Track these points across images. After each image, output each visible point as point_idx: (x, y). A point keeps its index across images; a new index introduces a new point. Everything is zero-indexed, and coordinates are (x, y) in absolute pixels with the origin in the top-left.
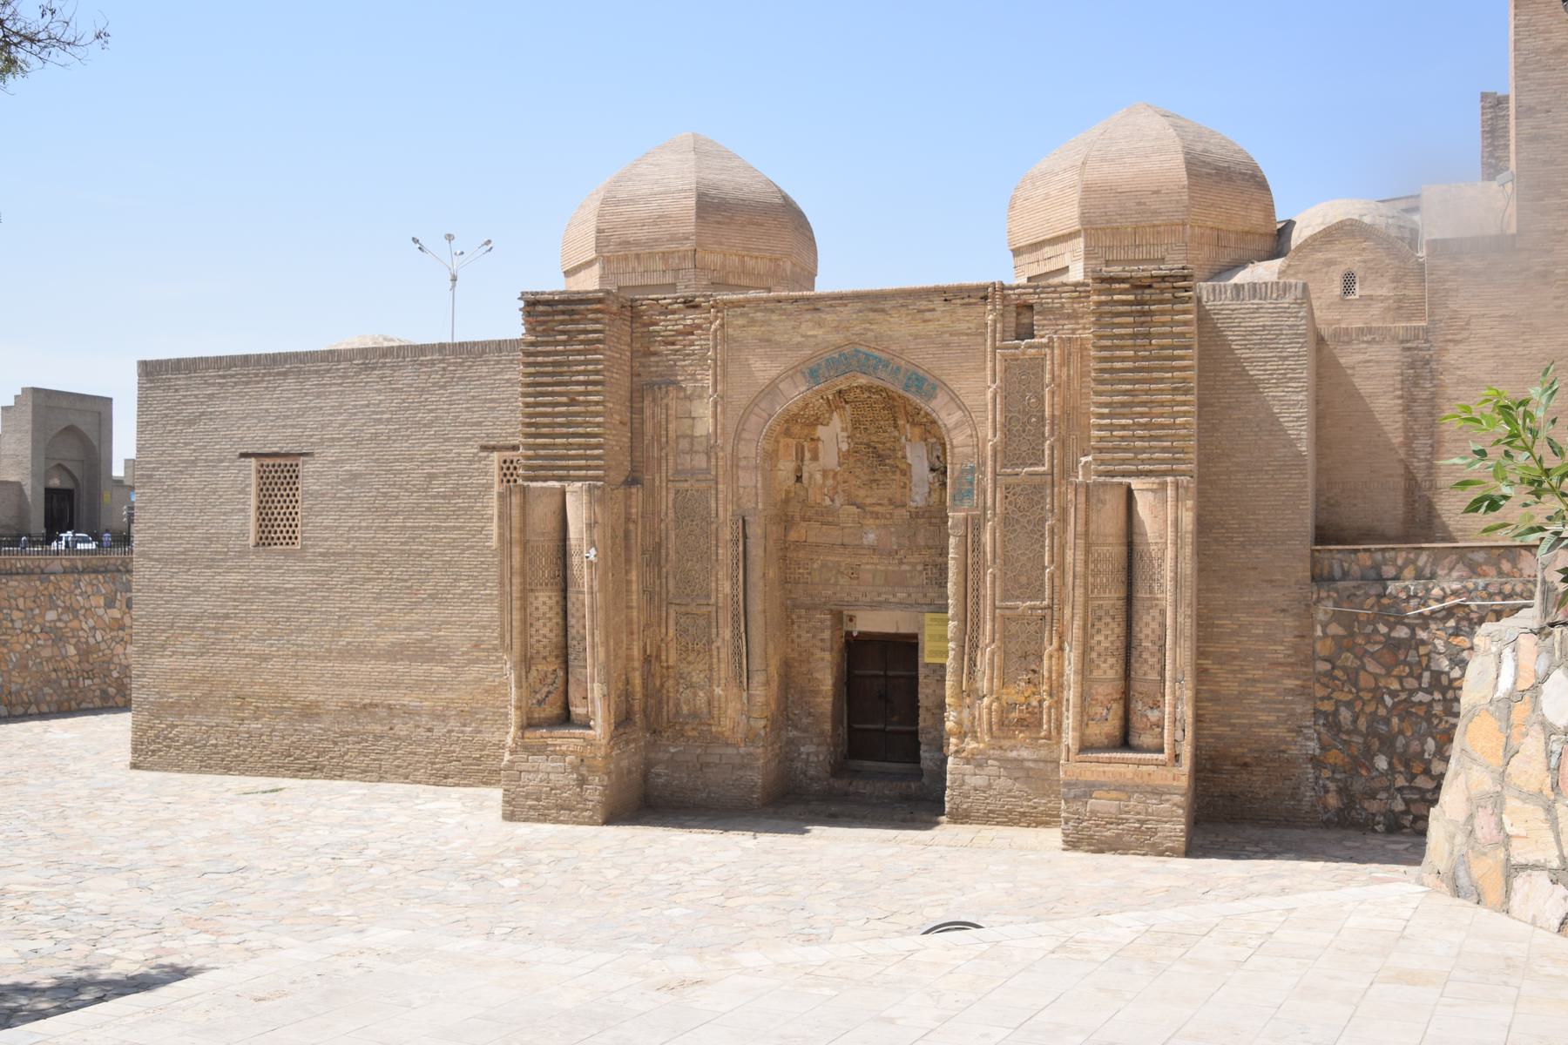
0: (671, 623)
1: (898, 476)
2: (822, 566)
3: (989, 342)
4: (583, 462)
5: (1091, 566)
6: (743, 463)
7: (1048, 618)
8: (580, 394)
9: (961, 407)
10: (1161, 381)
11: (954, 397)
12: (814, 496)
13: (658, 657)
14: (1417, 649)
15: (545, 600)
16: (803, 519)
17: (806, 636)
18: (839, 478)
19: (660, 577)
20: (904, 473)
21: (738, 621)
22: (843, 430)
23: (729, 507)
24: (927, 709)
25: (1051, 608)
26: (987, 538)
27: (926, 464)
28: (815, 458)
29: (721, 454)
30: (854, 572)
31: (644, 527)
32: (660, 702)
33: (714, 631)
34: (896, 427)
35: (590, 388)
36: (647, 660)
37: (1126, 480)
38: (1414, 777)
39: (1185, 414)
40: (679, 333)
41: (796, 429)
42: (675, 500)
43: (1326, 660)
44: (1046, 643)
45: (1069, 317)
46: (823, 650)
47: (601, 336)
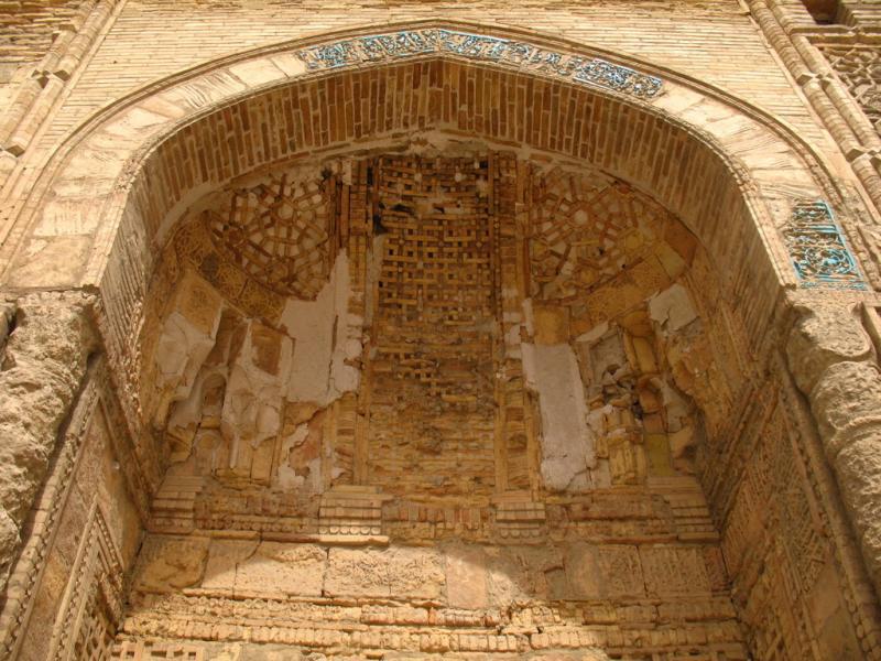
16: (203, 522)
22: (355, 307)
27: (578, 389)
28: (269, 363)
34: (495, 303)
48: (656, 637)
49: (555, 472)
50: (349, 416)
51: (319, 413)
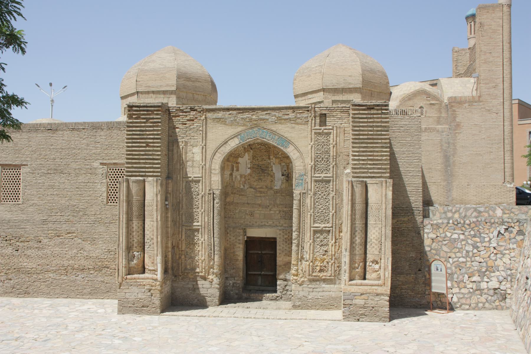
0: (184, 233)
1: (269, 178)
2: (240, 211)
3: (310, 127)
4: (152, 170)
5: (354, 212)
6: (213, 171)
7: (331, 231)
8: (151, 143)
9: (299, 151)
10: (377, 143)
11: (296, 148)
12: (236, 185)
13: (178, 247)
14: (461, 242)
15: (136, 224)
16: (232, 193)
17: (233, 238)
18: (247, 178)
20: (272, 177)
24: (280, 266)
25: (332, 227)
26: (308, 201)
28: (238, 170)
30: (252, 214)
31: (173, 196)
32: (178, 264)
34: (269, 159)
35: (155, 141)
36: (173, 248)
37: (365, 179)
38: (460, 289)
39: (386, 156)
40: (188, 120)
41: (231, 159)
42: (186, 186)
43: (429, 246)
44: (330, 240)
45: (340, 119)
46: (239, 243)
47: (160, 120)
48: (285, 209)
49: (275, 188)
50: (249, 177)
51: (245, 176)
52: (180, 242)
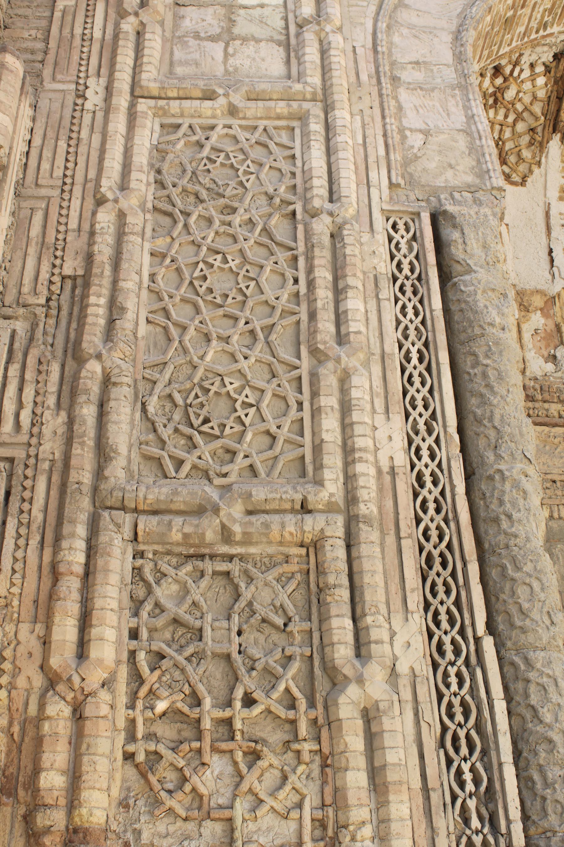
0: (111, 595)
19: (69, 393)
21: (456, 583)
23: (379, 177)
29: (337, 40)
33: (341, 626)
42: (160, 151)
52: (59, 709)
